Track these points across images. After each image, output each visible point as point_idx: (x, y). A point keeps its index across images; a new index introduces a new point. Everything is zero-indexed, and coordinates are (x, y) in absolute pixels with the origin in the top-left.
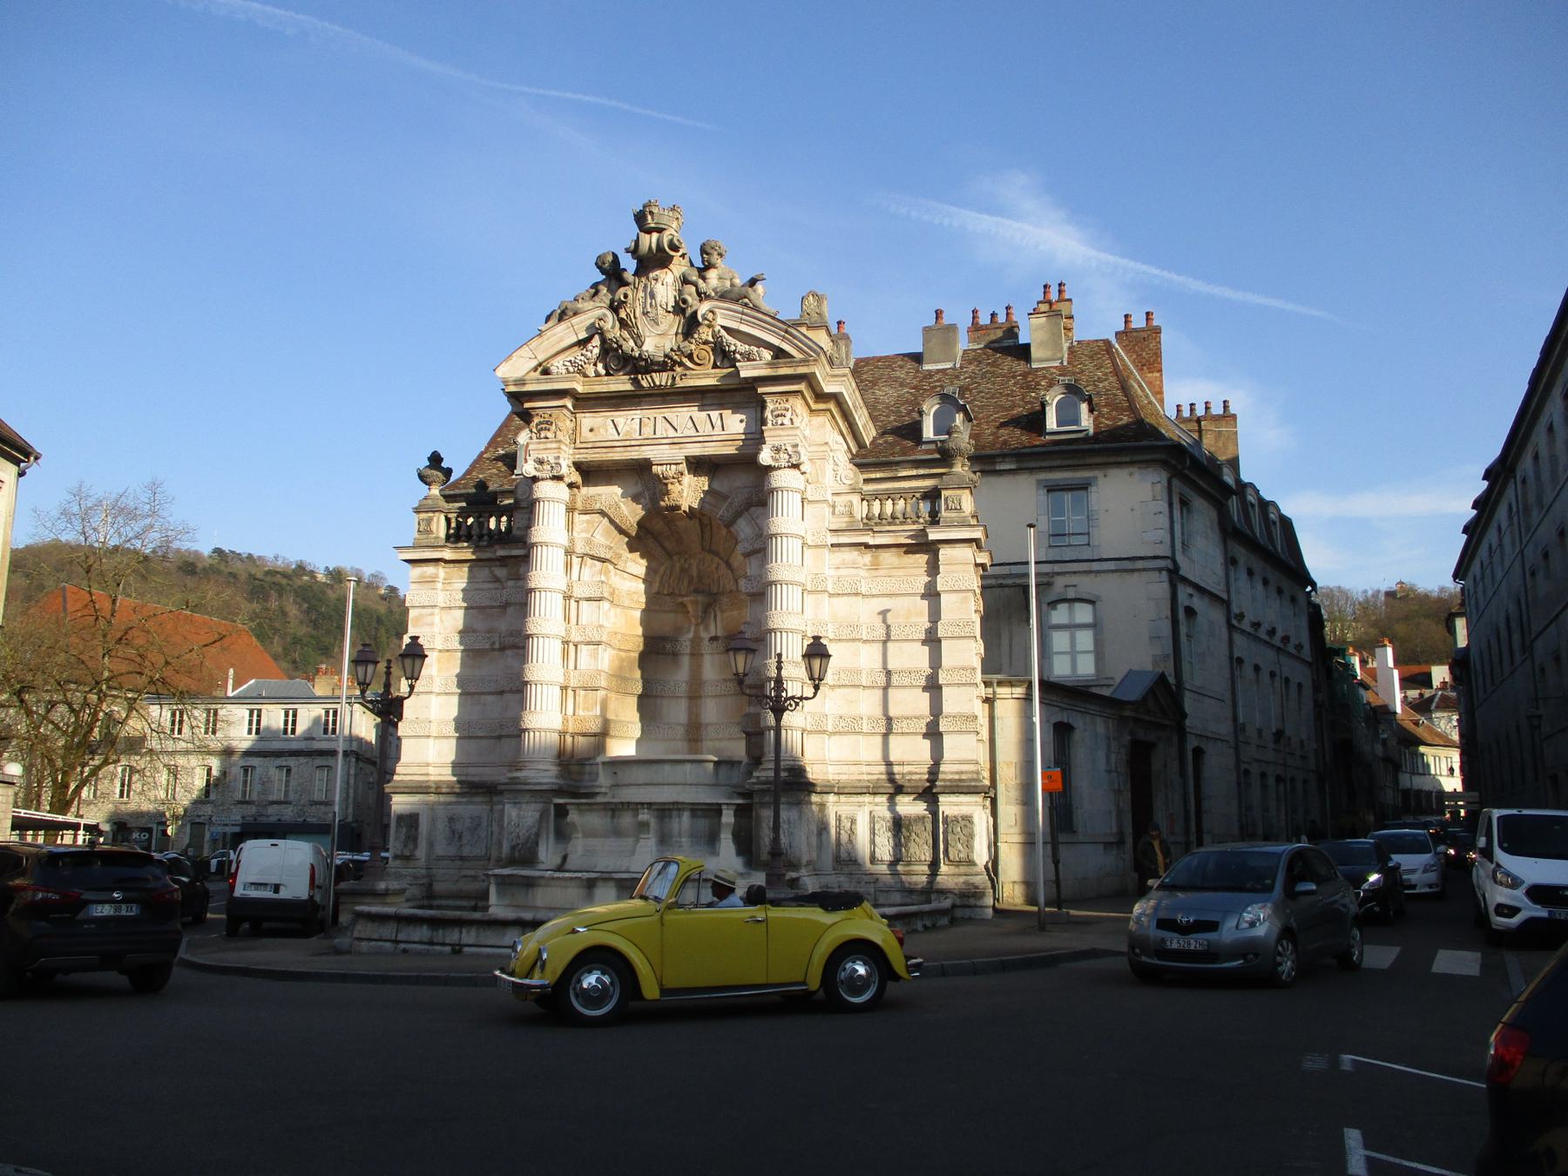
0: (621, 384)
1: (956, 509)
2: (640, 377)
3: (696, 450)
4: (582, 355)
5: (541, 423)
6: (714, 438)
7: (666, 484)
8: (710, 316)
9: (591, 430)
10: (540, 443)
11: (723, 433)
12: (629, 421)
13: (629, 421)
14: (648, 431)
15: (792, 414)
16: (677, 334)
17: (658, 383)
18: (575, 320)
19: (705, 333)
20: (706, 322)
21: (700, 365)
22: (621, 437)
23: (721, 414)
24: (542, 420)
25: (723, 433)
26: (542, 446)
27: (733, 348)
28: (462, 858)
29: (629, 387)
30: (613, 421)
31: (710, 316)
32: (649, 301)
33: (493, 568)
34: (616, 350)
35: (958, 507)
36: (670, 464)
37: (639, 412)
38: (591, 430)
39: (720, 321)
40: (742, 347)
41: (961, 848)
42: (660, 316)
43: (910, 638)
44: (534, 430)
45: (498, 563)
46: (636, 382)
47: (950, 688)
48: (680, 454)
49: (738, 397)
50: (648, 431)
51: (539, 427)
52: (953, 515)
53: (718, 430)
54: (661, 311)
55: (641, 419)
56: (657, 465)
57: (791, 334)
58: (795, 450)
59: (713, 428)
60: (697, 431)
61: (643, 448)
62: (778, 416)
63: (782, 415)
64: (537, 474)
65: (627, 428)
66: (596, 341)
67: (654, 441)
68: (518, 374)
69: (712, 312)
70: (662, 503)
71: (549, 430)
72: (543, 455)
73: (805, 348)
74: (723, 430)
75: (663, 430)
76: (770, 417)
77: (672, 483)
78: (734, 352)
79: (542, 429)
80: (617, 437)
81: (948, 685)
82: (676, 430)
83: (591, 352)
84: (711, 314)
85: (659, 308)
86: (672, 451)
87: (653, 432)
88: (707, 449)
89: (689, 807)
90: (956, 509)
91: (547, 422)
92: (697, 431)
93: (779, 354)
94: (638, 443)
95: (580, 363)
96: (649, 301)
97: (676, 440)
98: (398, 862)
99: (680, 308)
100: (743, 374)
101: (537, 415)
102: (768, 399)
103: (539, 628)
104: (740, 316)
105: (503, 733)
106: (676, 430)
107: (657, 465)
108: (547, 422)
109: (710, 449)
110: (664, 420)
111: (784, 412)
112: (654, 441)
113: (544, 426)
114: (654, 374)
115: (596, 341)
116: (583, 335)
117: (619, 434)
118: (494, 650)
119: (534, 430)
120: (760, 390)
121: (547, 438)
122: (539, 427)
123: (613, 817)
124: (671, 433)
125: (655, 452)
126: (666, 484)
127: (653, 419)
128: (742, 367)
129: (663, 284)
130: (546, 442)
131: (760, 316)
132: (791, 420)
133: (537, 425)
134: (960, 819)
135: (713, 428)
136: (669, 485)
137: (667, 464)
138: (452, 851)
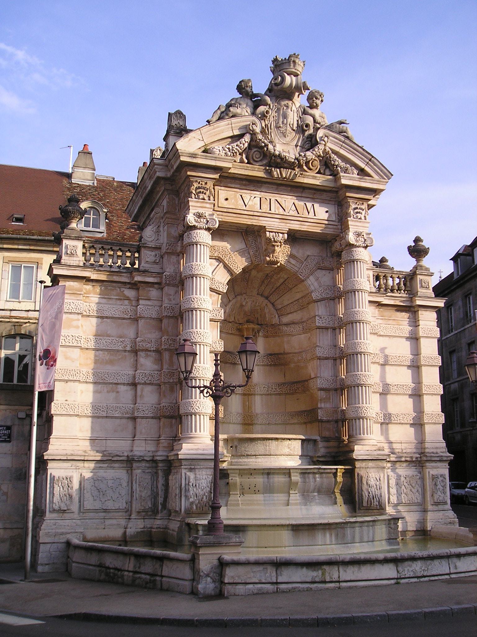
0: (257, 172)
1: (426, 288)
2: (273, 169)
3: (296, 226)
4: (237, 146)
5: (199, 188)
6: (309, 220)
7: (274, 246)
8: (326, 139)
9: (227, 199)
10: (198, 202)
11: (315, 217)
12: (252, 198)
13: (252, 198)
14: (265, 208)
15: (365, 214)
16: (296, 146)
17: (284, 176)
18: (234, 120)
19: (320, 149)
20: (324, 143)
21: (310, 169)
22: (247, 209)
23: (313, 205)
24: (200, 185)
25: (315, 217)
26: (199, 205)
27: (337, 163)
28: (105, 511)
29: (261, 174)
30: (241, 196)
31: (326, 139)
32: (281, 120)
33: (122, 289)
34: (262, 148)
35: (428, 287)
36: (278, 233)
37: (258, 193)
38: (227, 199)
39: (329, 145)
40: (342, 164)
41: (440, 494)
42: (288, 131)
43: (402, 364)
44: (194, 192)
45: (128, 286)
46: (270, 173)
47: (428, 396)
48: (286, 227)
49: (324, 196)
50: (265, 208)
51: (198, 190)
52: (424, 291)
53: (311, 215)
54: (289, 129)
55: (260, 198)
56: (269, 232)
57: (373, 163)
58: (368, 236)
59: (309, 213)
60: (298, 213)
61: (261, 218)
62: (357, 213)
63: (359, 213)
64: (197, 224)
65: (250, 203)
66: (247, 138)
67: (270, 215)
68: (192, 150)
69: (327, 137)
70: (268, 259)
71: (205, 194)
72: (201, 211)
73: (379, 171)
74: (315, 216)
75: (275, 208)
76: (352, 212)
77: (277, 246)
78: (337, 166)
79: (200, 192)
80: (244, 208)
81: (427, 394)
82: (285, 210)
83: (244, 145)
84: (326, 138)
85: (288, 125)
86: (280, 224)
87: (269, 209)
88: (303, 227)
89: (300, 471)
90: (426, 288)
91: (204, 188)
92: (298, 213)
93: (362, 172)
94: (258, 214)
95: (236, 151)
96: (281, 120)
97: (284, 217)
98: (54, 515)
99: (301, 129)
100: (344, 182)
101: (196, 181)
102: (350, 201)
103: (202, 338)
104: (342, 143)
105: (139, 415)
106: (285, 210)
107: (269, 232)
108: (204, 188)
109: (305, 227)
110: (276, 202)
111: (361, 211)
112: (270, 215)
113: (202, 190)
114: (282, 169)
115: (247, 138)
116: (237, 132)
117: (246, 206)
118: (125, 351)
119: (194, 192)
120: (348, 194)
121: (204, 199)
122: (198, 190)
123: (268, 478)
124: (281, 211)
125: (269, 223)
126: (274, 246)
127: (269, 200)
128: (343, 176)
129: (291, 111)
130: (203, 202)
131: (355, 146)
132: (365, 217)
133: (197, 188)
134: (439, 476)
135: (309, 213)
136: (276, 247)
137: (275, 232)
138: (98, 505)
